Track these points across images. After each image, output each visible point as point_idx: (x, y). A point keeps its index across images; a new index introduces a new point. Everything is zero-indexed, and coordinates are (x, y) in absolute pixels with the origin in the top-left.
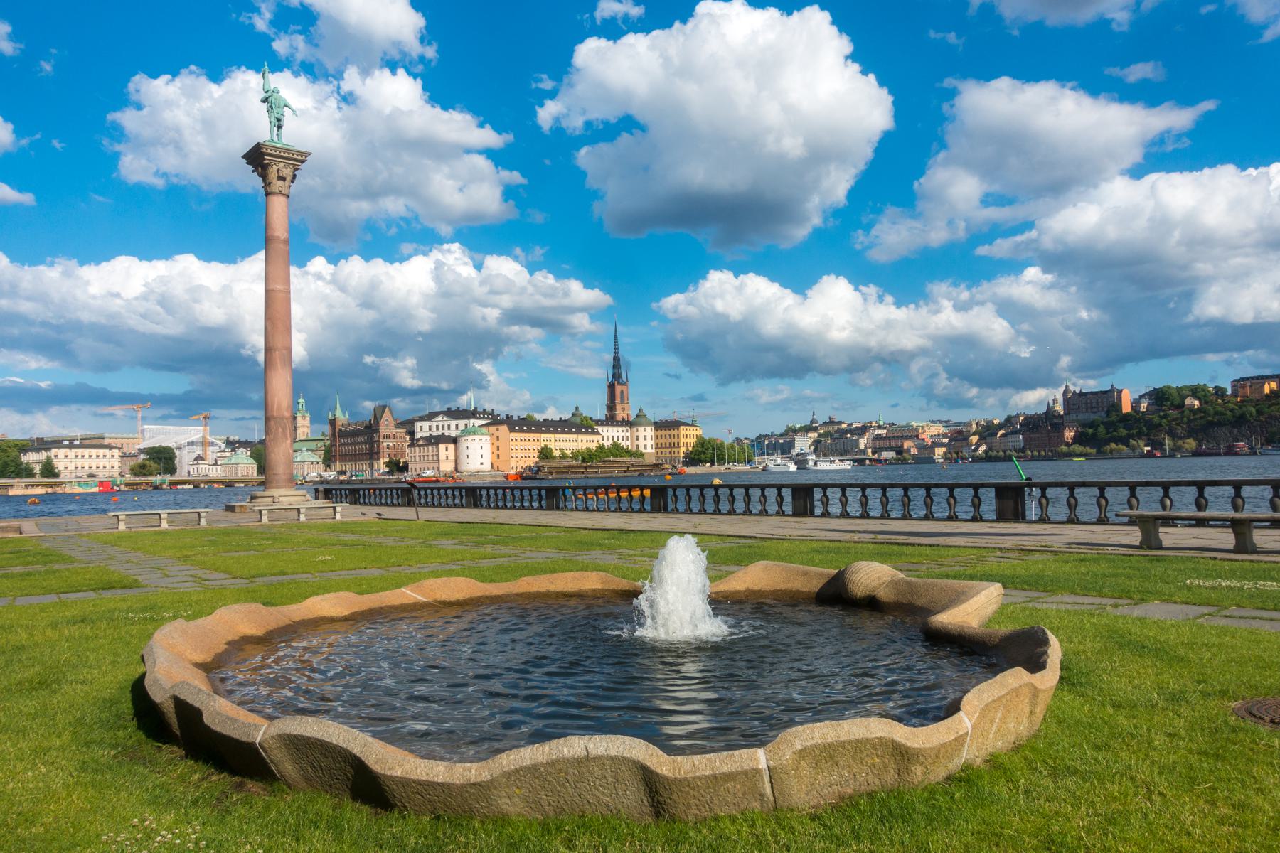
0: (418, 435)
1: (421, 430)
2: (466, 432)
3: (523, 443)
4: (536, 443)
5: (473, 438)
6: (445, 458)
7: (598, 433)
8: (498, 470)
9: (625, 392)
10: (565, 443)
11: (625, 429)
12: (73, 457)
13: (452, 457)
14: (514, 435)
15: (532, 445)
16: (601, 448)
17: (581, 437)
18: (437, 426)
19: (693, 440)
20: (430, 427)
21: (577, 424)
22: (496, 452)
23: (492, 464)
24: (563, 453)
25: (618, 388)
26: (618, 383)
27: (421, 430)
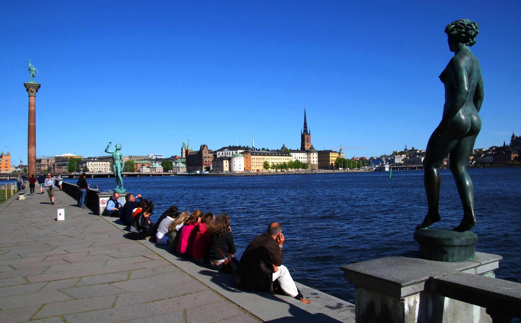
0: (218, 157)
3: (257, 160)
4: (263, 160)
5: (239, 158)
6: (225, 166)
7: (291, 156)
9: (309, 138)
10: (274, 160)
11: (305, 154)
12: (94, 165)
13: (228, 166)
17: (283, 157)
18: (225, 153)
19: (335, 159)
20: (222, 153)
21: (284, 152)
22: (246, 164)
23: (244, 168)
24: (273, 164)
25: (306, 136)
26: (306, 134)
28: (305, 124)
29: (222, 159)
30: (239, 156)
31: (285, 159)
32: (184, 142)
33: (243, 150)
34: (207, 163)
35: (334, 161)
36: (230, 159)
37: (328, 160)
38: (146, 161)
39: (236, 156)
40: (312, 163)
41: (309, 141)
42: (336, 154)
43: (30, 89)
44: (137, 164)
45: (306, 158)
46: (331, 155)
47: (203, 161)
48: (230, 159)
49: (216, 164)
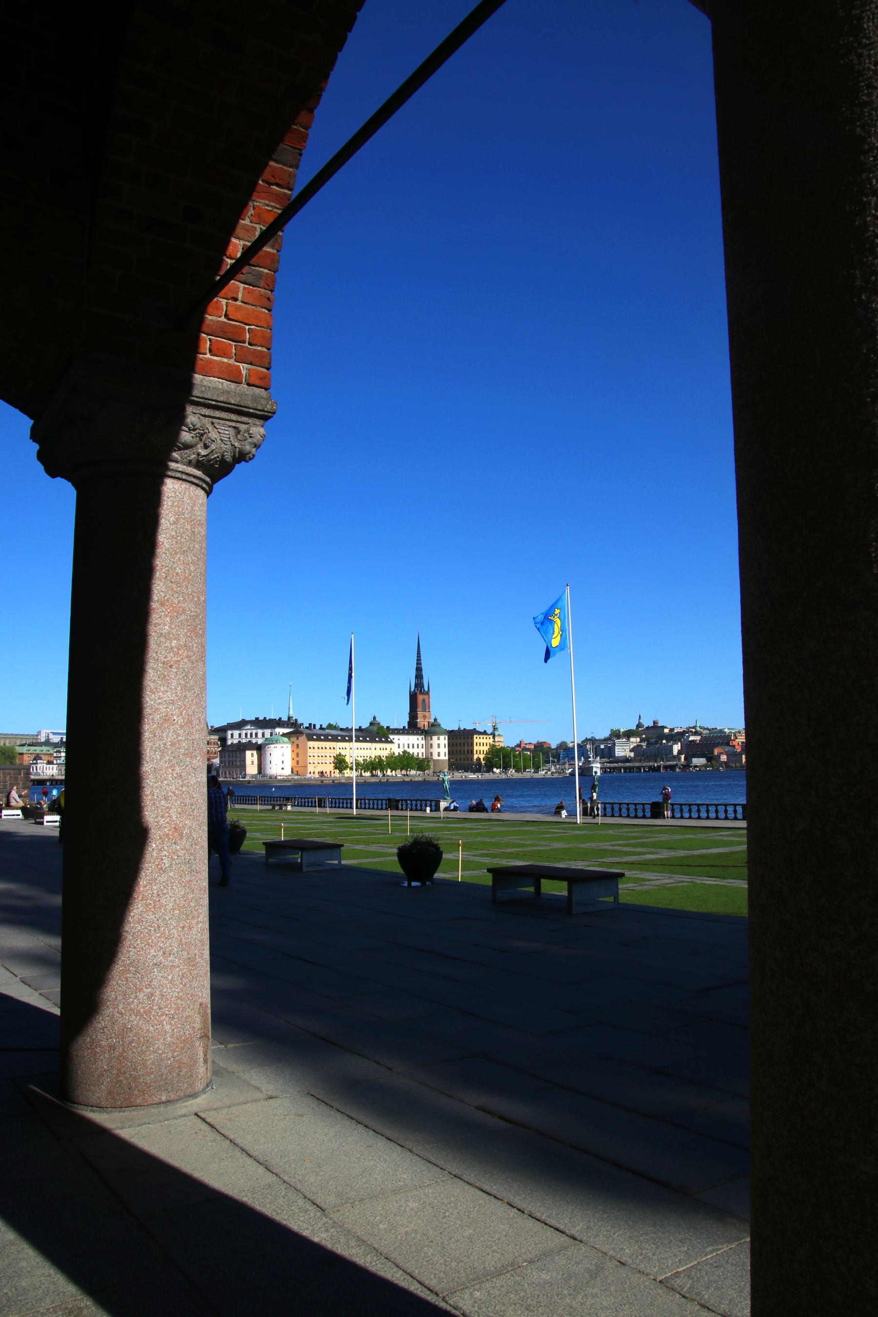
0: (229, 742)
3: (320, 750)
4: (332, 750)
6: (251, 763)
7: (391, 742)
8: (297, 774)
9: (427, 701)
11: (420, 737)
13: (256, 762)
15: (328, 752)
16: (391, 756)
18: (246, 734)
20: (240, 735)
23: (292, 769)
25: (420, 698)
26: (421, 691)
28: (419, 670)
29: (242, 748)
30: (281, 741)
31: (378, 749)
33: (287, 727)
35: (482, 753)
36: (260, 748)
37: (470, 751)
38: (45, 749)
39: (274, 742)
40: (435, 757)
41: (426, 707)
42: (488, 738)
44: (22, 754)
45: (423, 747)
46: (477, 739)
48: (260, 748)
49: (227, 759)
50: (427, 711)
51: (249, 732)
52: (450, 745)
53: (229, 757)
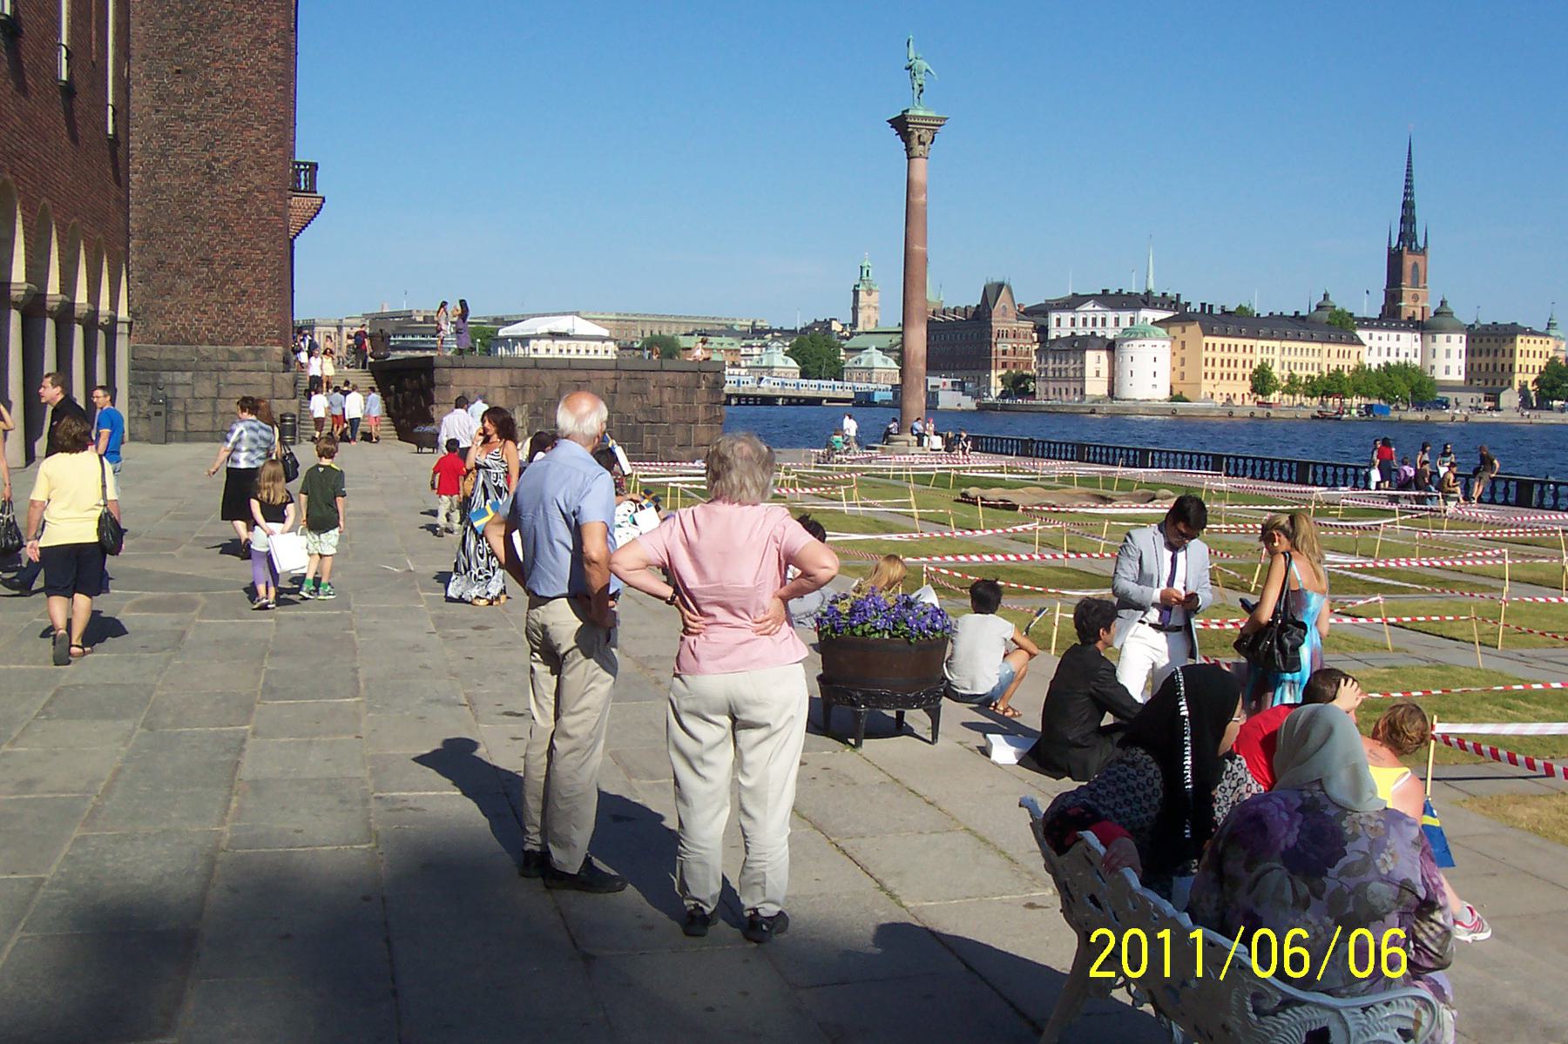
0: (1052, 335)
1: (1059, 325)
2: (1132, 334)
5: (1142, 342)
13: (1105, 373)
14: (1209, 340)
16: (1360, 370)
18: (1085, 321)
20: (1073, 320)
23: (1171, 387)
25: (1409, 260)
26: (1410, 248)
27: (1059, 325)
28: (1408, 206)
29: (1077, 346)
30: (1153, 334)
32: (865, 264)
33: (1161, 308)
34: (1009, 358)
35: (1530, 370)
36: (1111, 347)
37: (1507, 368)
39: (1139, 335)
43: (917, 134)
46: (1521, 343)
47: (994, 349)
50: (1421, 285)
51: (1090, 317)
52: (1470, 352)
53: (1054, 362)
